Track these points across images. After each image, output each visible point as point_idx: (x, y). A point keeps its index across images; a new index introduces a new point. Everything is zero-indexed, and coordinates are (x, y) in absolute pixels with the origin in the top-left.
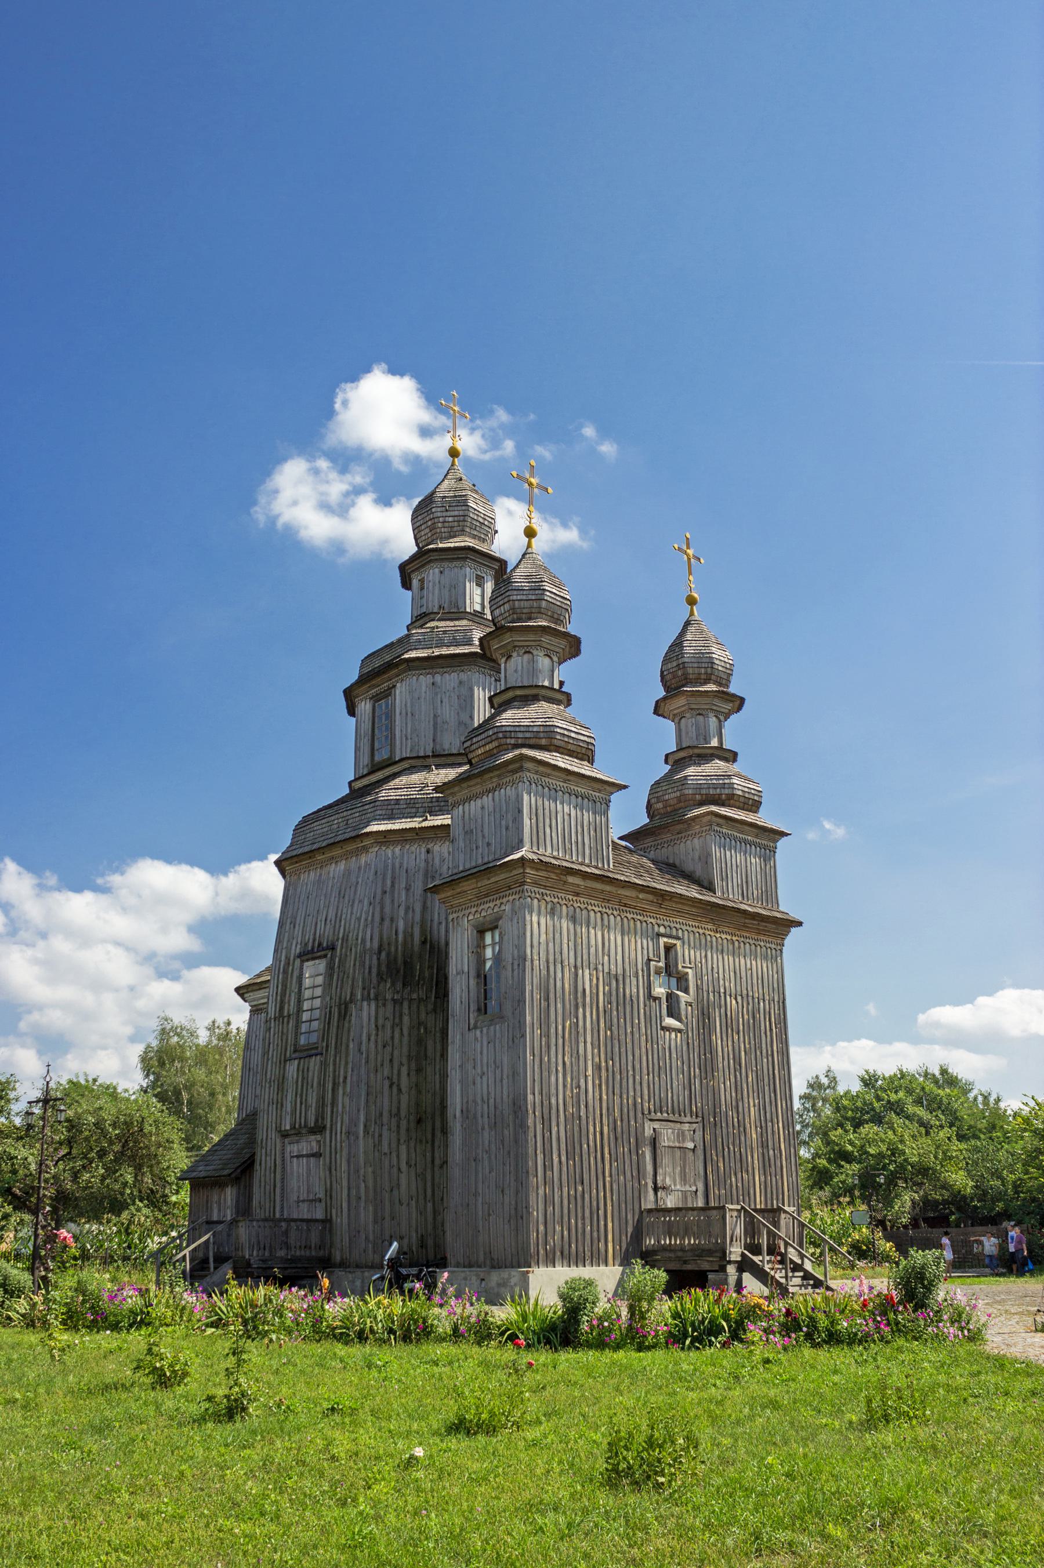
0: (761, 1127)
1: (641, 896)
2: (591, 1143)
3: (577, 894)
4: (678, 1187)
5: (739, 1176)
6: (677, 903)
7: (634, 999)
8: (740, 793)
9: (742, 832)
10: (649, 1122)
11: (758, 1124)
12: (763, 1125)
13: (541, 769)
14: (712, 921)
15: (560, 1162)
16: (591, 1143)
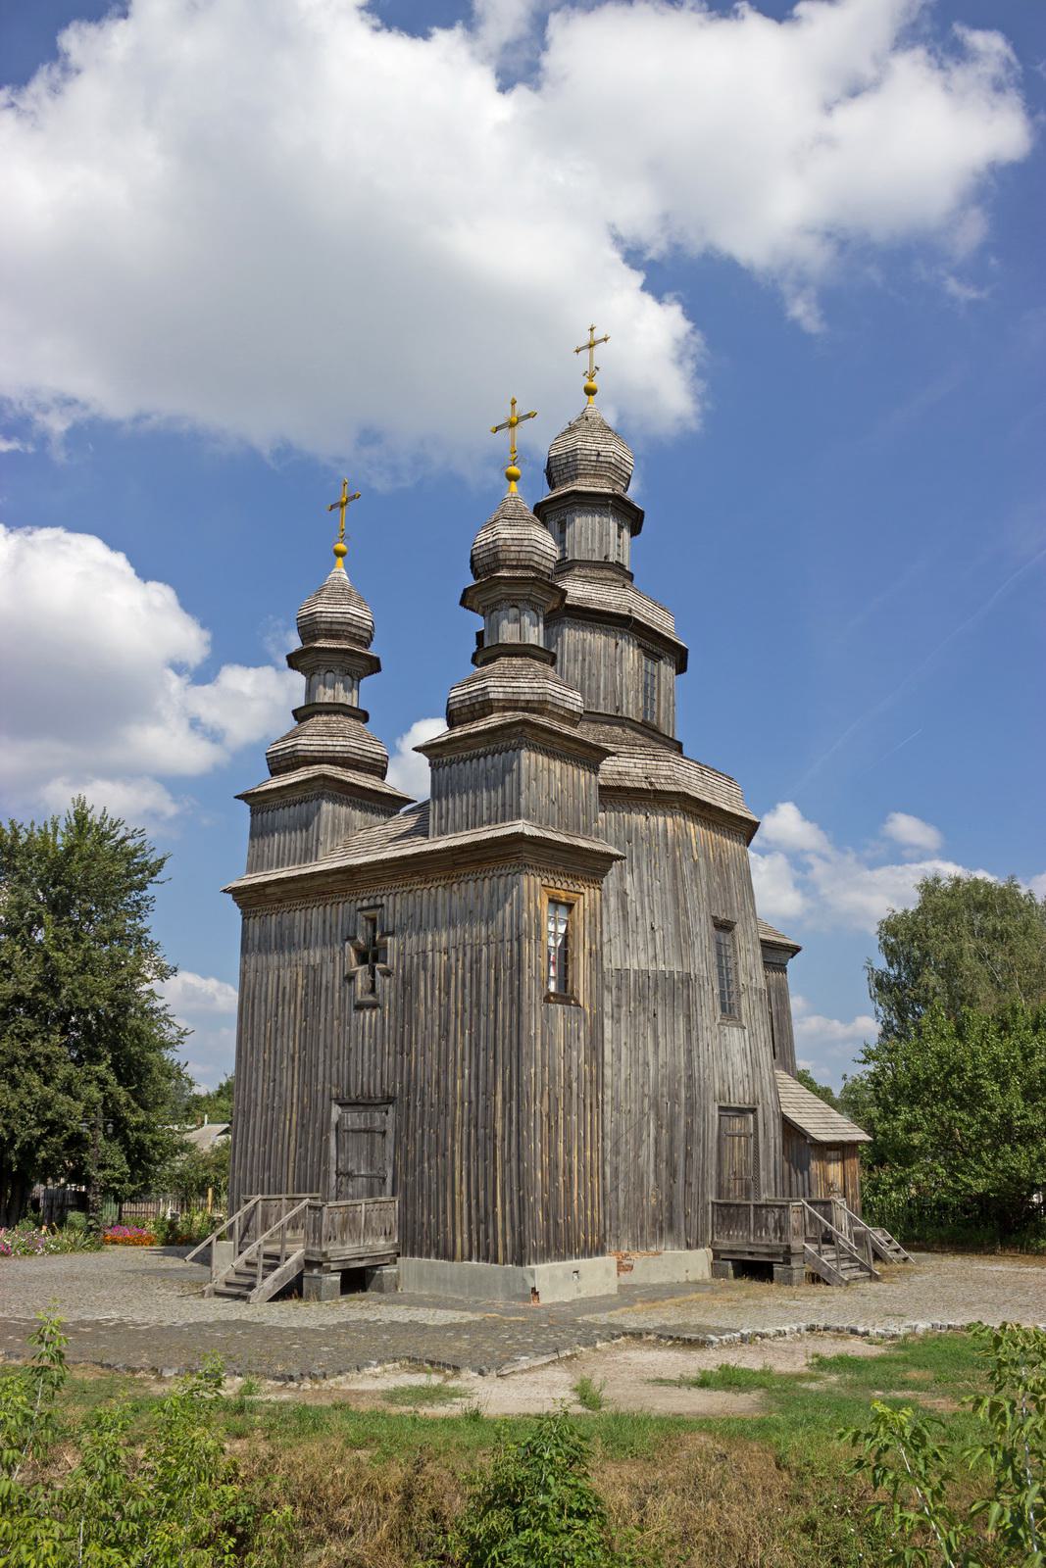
0: (470, 1103)
1: (330, 880)
2: (281, 1132)
3: (280, 901)
4: (363, 1173)
5: (433, 1162)
6: (367, 872)
7: (330, 985)
8: (458, 706)
9: (469, 748)
10: (337, 1106)
11: (466, 1098)
12: (473, 1098)
13: (259, 798)
14: (417, 873)
15: (253, 1149)
16: (281, 1132)
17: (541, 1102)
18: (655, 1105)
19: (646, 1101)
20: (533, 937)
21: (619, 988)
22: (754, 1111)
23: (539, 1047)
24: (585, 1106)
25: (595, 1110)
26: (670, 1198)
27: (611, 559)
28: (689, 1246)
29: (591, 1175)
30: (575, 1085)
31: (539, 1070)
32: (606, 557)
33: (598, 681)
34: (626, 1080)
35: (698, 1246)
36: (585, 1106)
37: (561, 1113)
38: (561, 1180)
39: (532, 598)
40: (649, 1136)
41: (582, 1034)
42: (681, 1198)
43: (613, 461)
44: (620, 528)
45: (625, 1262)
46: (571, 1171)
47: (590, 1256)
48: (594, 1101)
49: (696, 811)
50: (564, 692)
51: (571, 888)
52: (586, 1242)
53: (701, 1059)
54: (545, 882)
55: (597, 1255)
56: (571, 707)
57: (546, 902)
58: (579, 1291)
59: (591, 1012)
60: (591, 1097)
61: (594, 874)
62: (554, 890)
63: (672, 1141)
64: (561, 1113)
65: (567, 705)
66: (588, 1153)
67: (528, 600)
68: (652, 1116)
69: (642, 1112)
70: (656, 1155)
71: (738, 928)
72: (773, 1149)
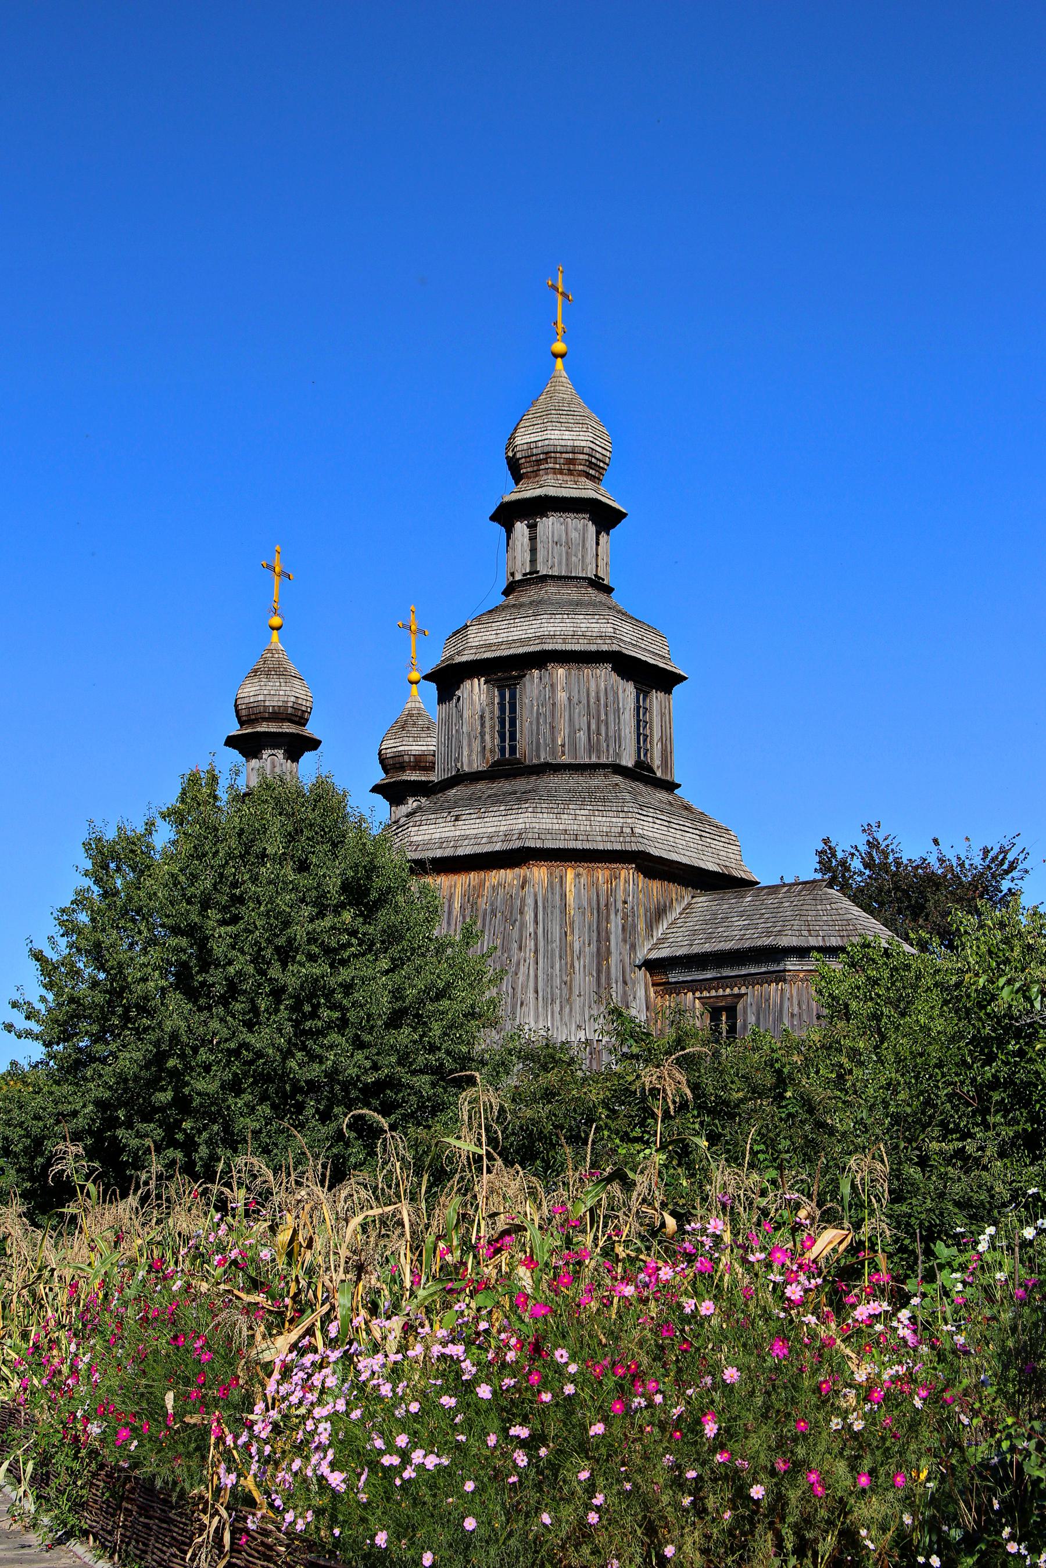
44: (532, 527)
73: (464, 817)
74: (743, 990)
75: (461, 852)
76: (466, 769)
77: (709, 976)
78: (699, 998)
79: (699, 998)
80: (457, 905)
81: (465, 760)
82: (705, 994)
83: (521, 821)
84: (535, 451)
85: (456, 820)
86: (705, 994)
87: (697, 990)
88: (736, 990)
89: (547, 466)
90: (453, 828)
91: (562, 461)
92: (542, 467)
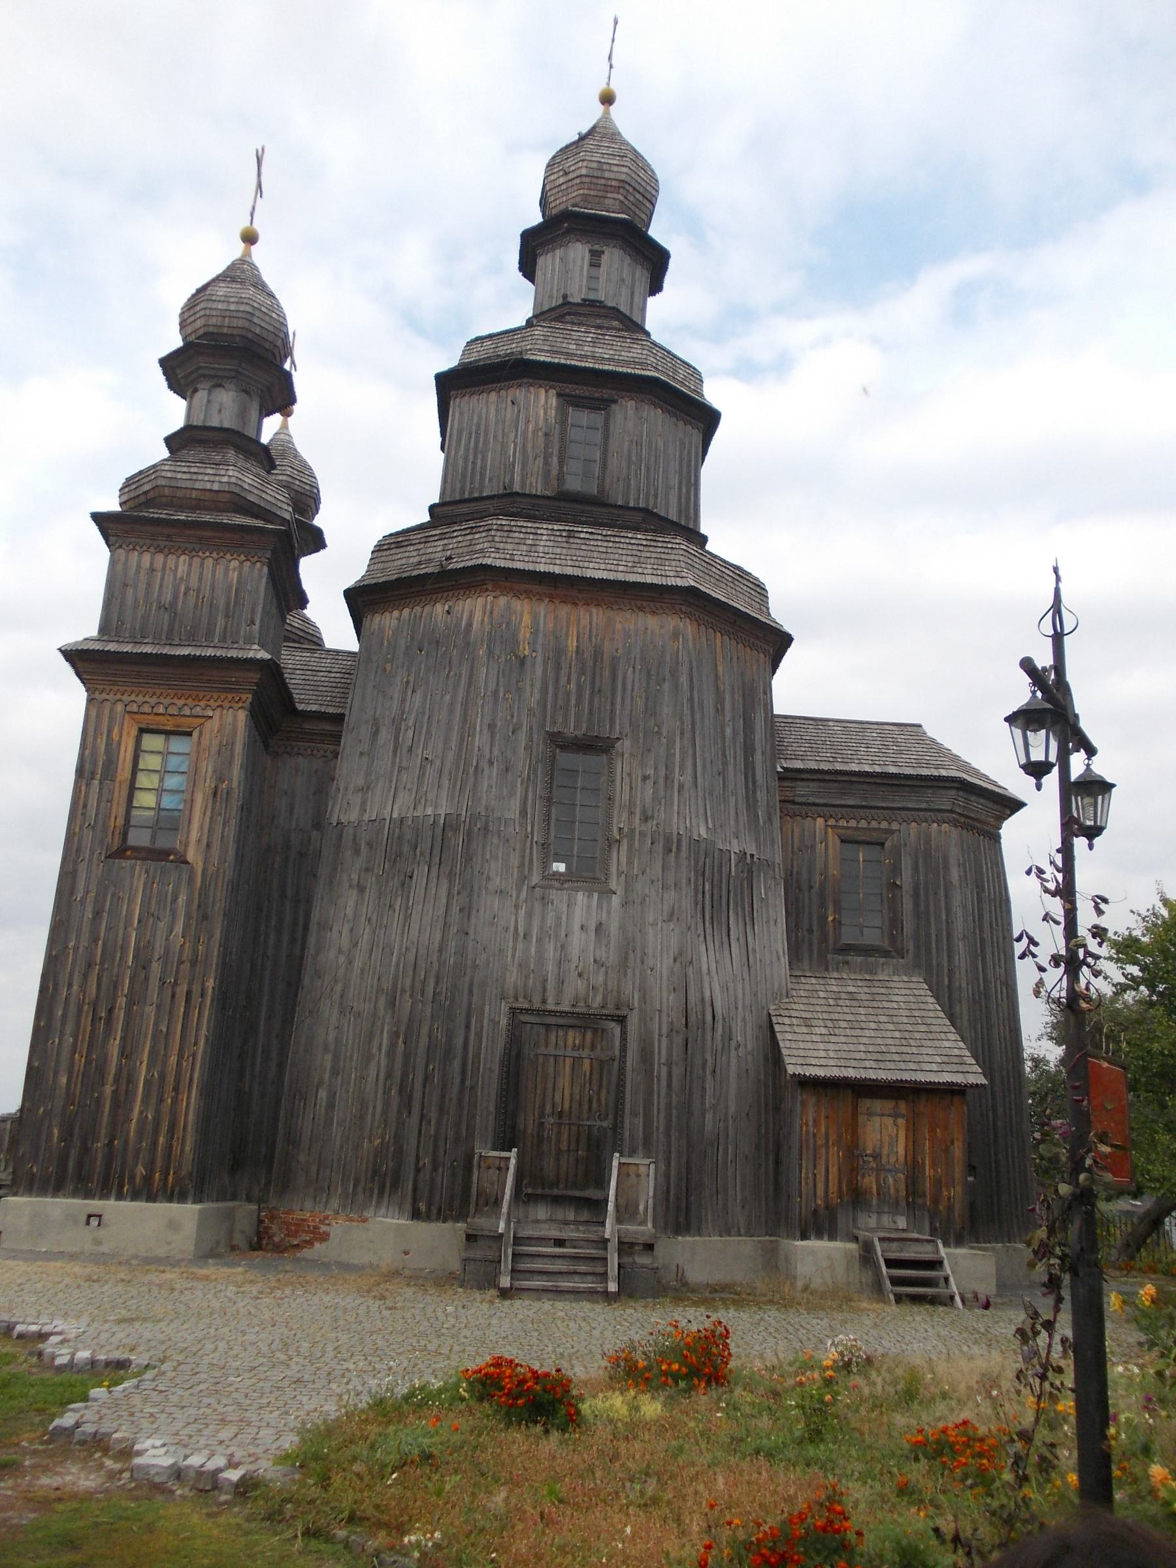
17: (83, 988)
18: (392, 1004)
19: (382, 1000)
20: (98, 777)
21: (369, 845)
22: (622, 1020)
23: (89, 914)
24: (173, 996)
25: (196, 999)
26: (398, 1138)
27: (571, 300)
28: (416, 1215)
29: (176, 1089)
30: (156, 967)
31: (84, 943)
32: (565, 297)
33: (484, 460)
34: (362, 970)
35: (442, 1215)
36: (173, 996)
37: (122, 1001)
38: (108, 1089)
39: (207, 372)
40: (380, 1049)
41: (182, 899)
42: (413, 1142)
43: (584, 171)
44: (596, 255)
45: (324, 1228)
46: (131, 1080)
47: (151, 1198)
48: (196, 989)
49: (537, 588)
50: (192, 470)
51: (187, 711)
52: (148, 1179)
53: (472, 936)
54: (134, 708)
55: (170, 1199)
56: (208, 486)
57: (134, 732)
58: (97, 1242)
59: (204, 870)
60: (190, 984)
61: (230, 690)
62: (151, 717)
63: (407, 1055)
64: (122, 1001)
65: (198, 485)
66: (173, 1059)
67: (204, 376)
68: (387, 1020)
69: (375, 1015)
70: (389, 1076)
71: (625, 745)
72: (664, 1083)
73: (582, 535)
74: (895, 826)
75: (589, 574)
76: (517, 488)
77: (851, 802)
78: (832, 827)
79: (832, 827)
80: (572, 644)
81: (517, 478)
82: (843, 823)
83: (672, 557)
84: (607, 175)
85: (569, 537)
86: (843, 823)
87: (831, 816)
88: (884, 825)
89: (616, 196)
90: (565, 545)
91: (631, 199)
92: (609, 195)
